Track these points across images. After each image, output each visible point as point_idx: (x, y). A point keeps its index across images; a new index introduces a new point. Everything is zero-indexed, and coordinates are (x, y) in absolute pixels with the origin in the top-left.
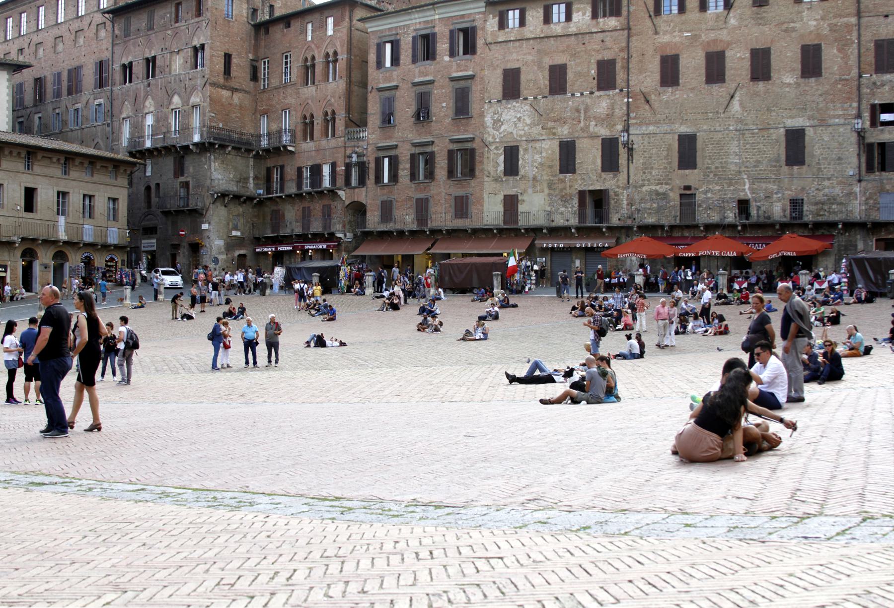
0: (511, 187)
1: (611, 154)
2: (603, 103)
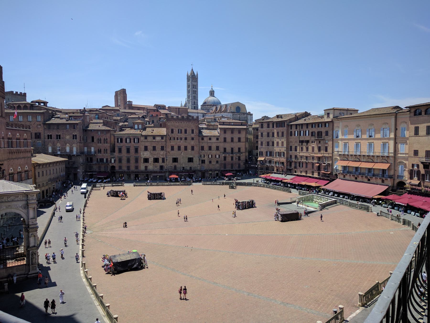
0: (146, 164)
1: (163, 159)
2: (162, 152)
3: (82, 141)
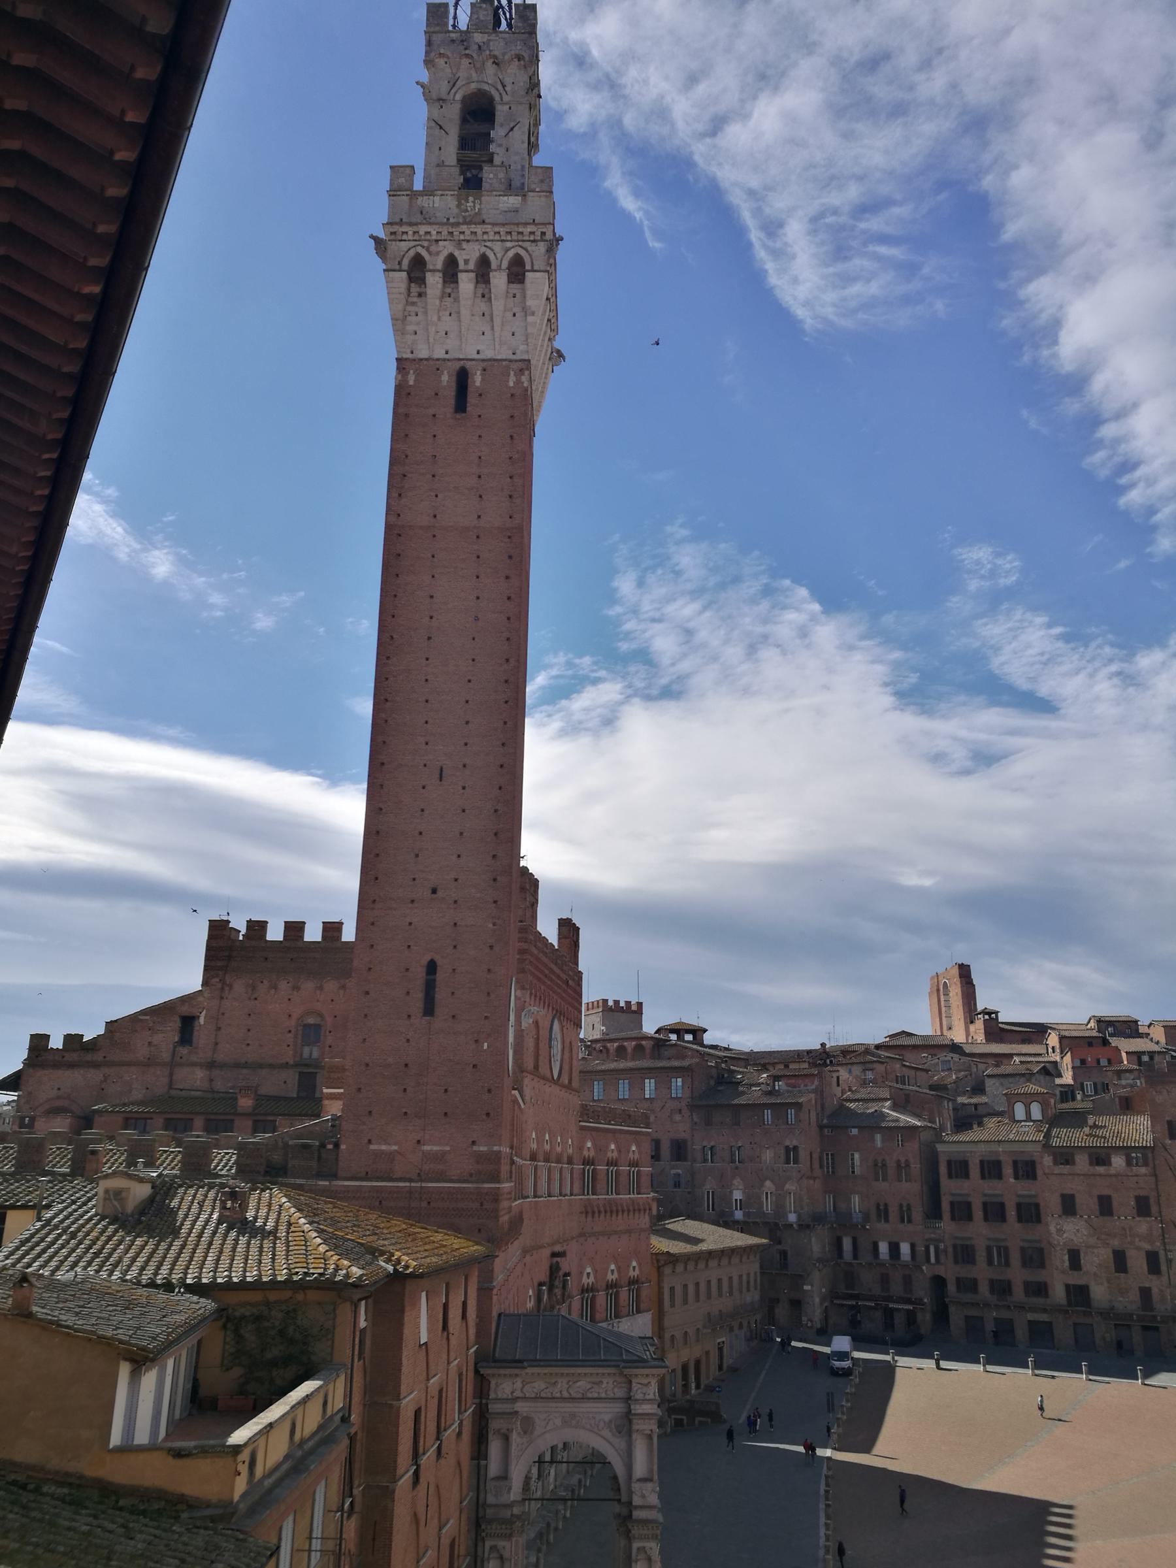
2: (1143, 1226)
3: (818, 1172)
